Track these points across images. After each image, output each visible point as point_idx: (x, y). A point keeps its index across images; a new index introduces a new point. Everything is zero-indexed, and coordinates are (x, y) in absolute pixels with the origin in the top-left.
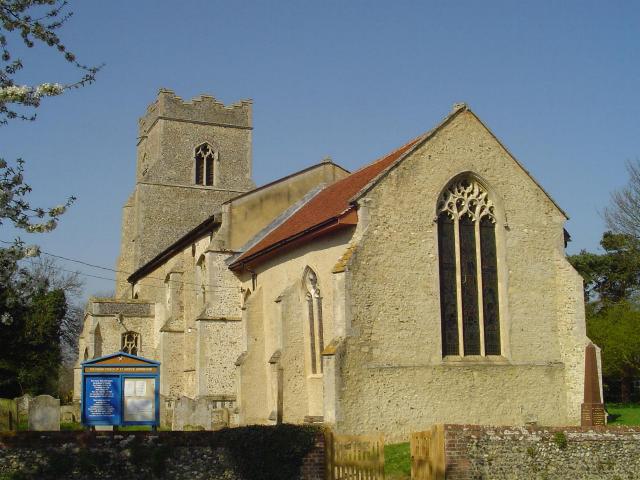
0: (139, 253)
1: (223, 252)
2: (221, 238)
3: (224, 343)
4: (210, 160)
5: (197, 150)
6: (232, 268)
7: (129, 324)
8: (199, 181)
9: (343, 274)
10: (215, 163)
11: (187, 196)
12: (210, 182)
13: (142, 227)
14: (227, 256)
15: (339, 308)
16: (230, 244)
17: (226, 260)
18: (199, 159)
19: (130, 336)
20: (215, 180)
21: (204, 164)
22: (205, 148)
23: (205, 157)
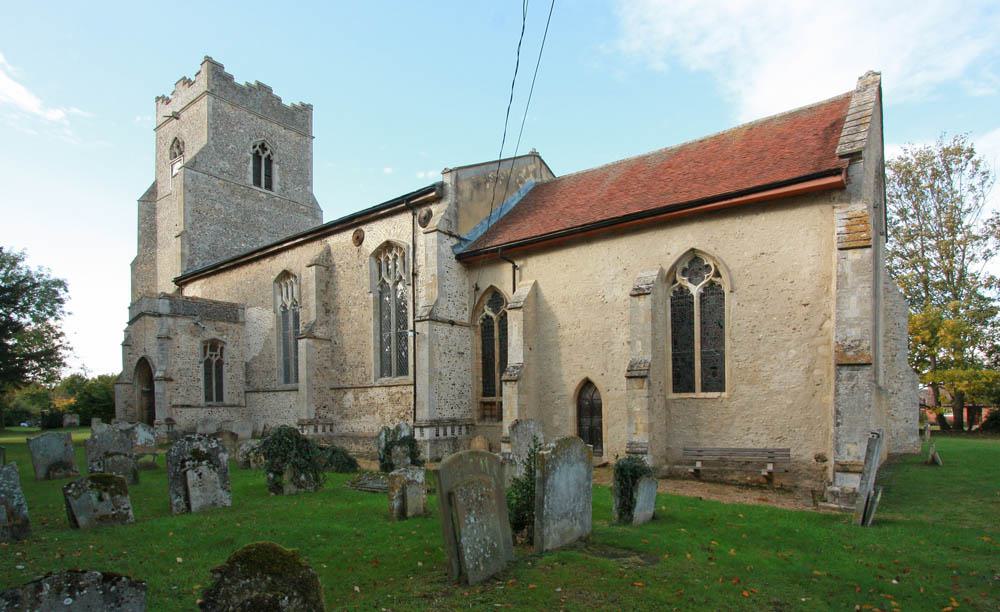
0: (187, 251)
1: (450, 235)
2: (447, 217)
3: (453, 353)
4: (269, 161)
5: (254, 147)
6: (460, 258)
7: (212, 334)
8: (257, 182)
9: (868, 251)
10: (276, 168)
11: (244, 197)
12: (269, 186)
13: (190, 221)
14: (455, 241)
15: (853, 300)
16: (457, 227)
17: (453, 247)
18: (257, 157)
19: (213, 345)
20: (276, 186)
21: (262, 163)
22: (263, 147)
23: (264, 157)
